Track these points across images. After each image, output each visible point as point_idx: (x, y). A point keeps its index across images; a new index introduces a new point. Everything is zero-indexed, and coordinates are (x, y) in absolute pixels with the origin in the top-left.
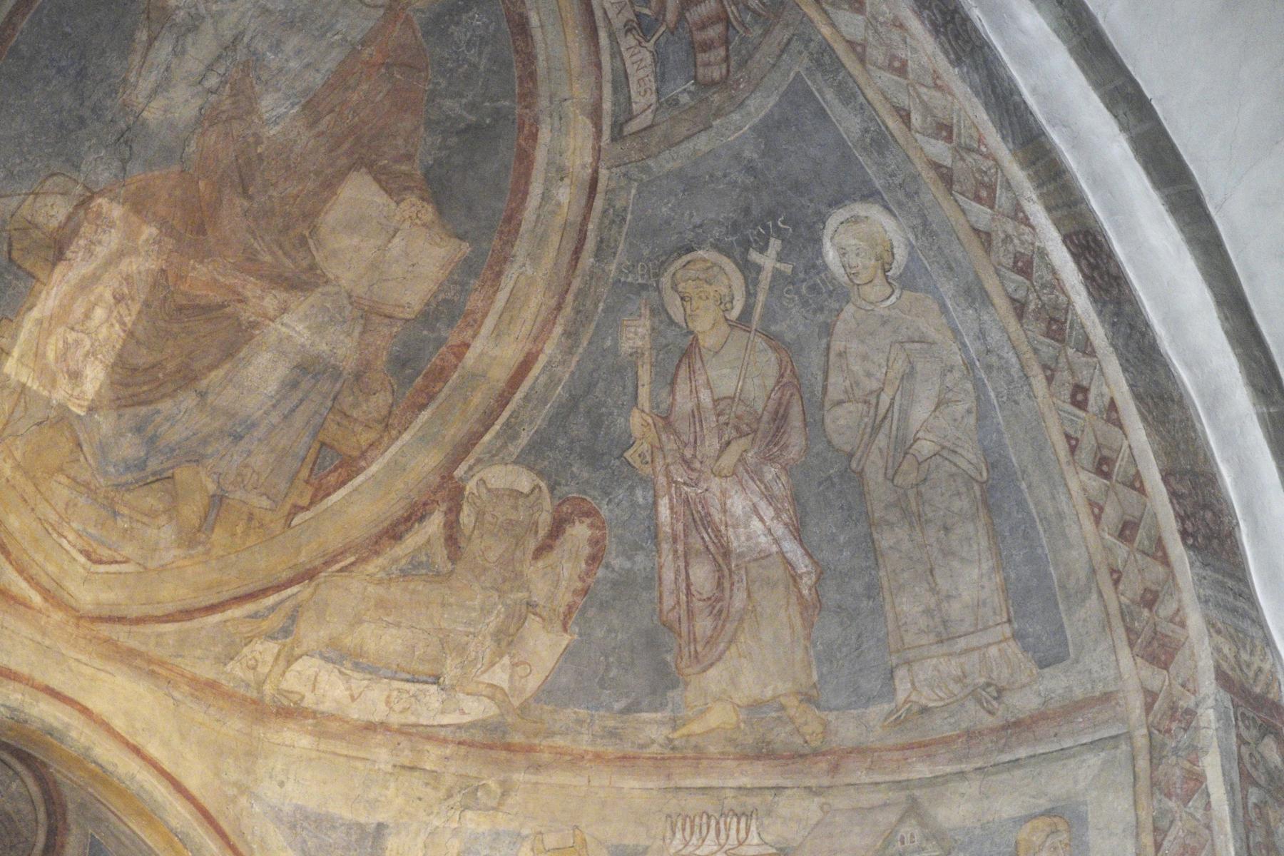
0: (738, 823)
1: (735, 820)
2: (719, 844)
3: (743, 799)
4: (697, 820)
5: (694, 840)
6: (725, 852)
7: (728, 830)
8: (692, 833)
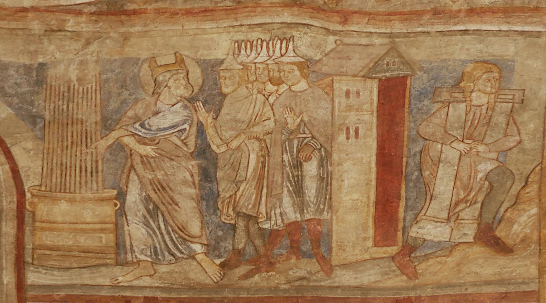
0: (281, 44)
1: (279, 42)
2: (269, 56)
3: (285, 30)
4: (255, 43)
5: (253, 55)
6: (273, 60)
7: (274, 47)
8: (251, 50)
